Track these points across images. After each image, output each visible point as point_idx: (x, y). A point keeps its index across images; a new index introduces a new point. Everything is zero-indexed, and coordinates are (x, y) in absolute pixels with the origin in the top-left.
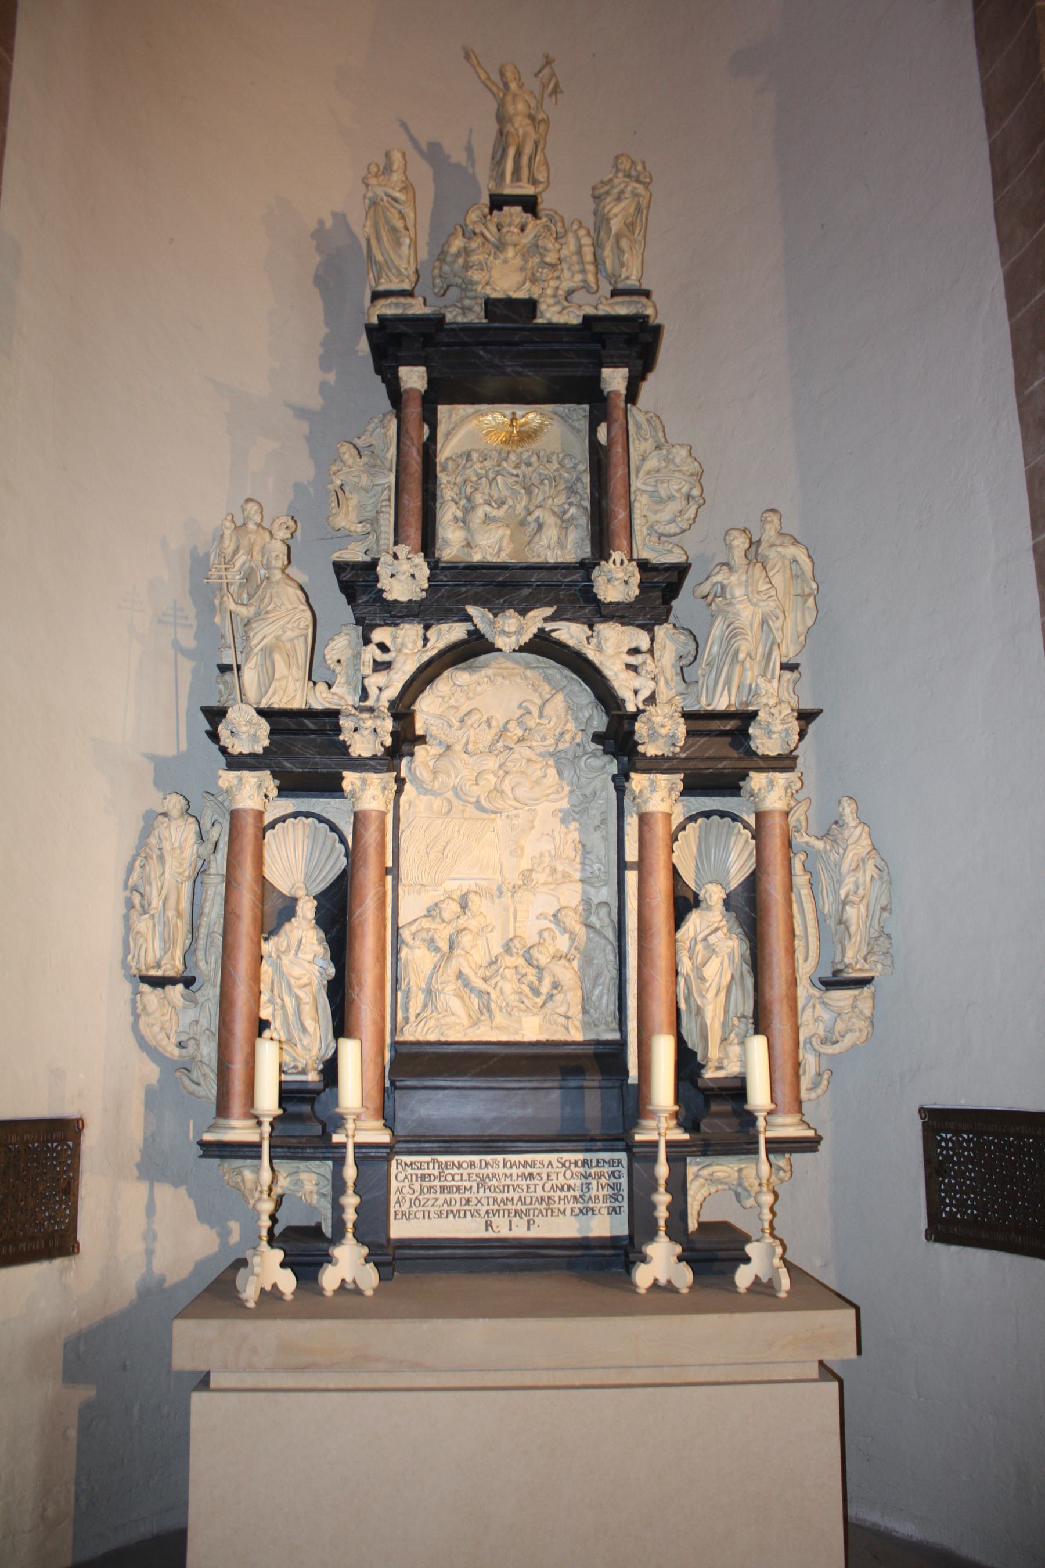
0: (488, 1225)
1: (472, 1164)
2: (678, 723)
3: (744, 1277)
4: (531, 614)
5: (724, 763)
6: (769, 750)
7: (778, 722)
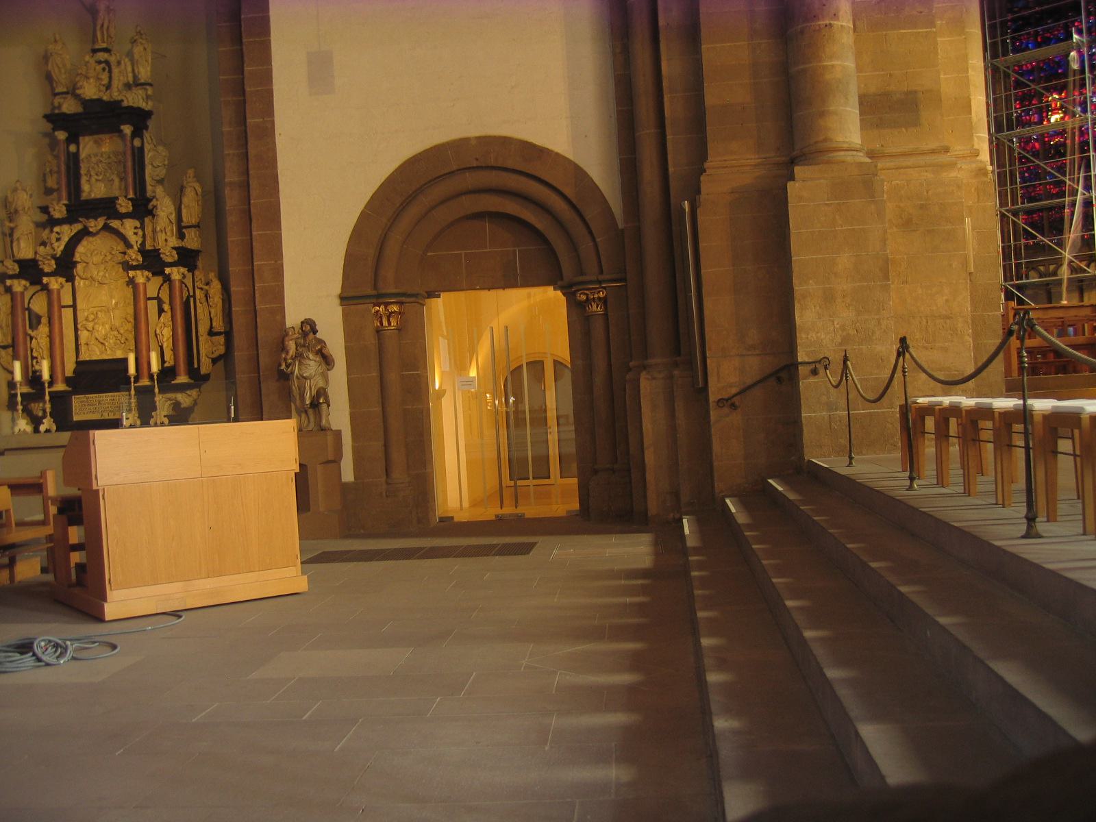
0: (102, 415)
1: (96, 397)
3: (152, 422)
4: (99, 219)
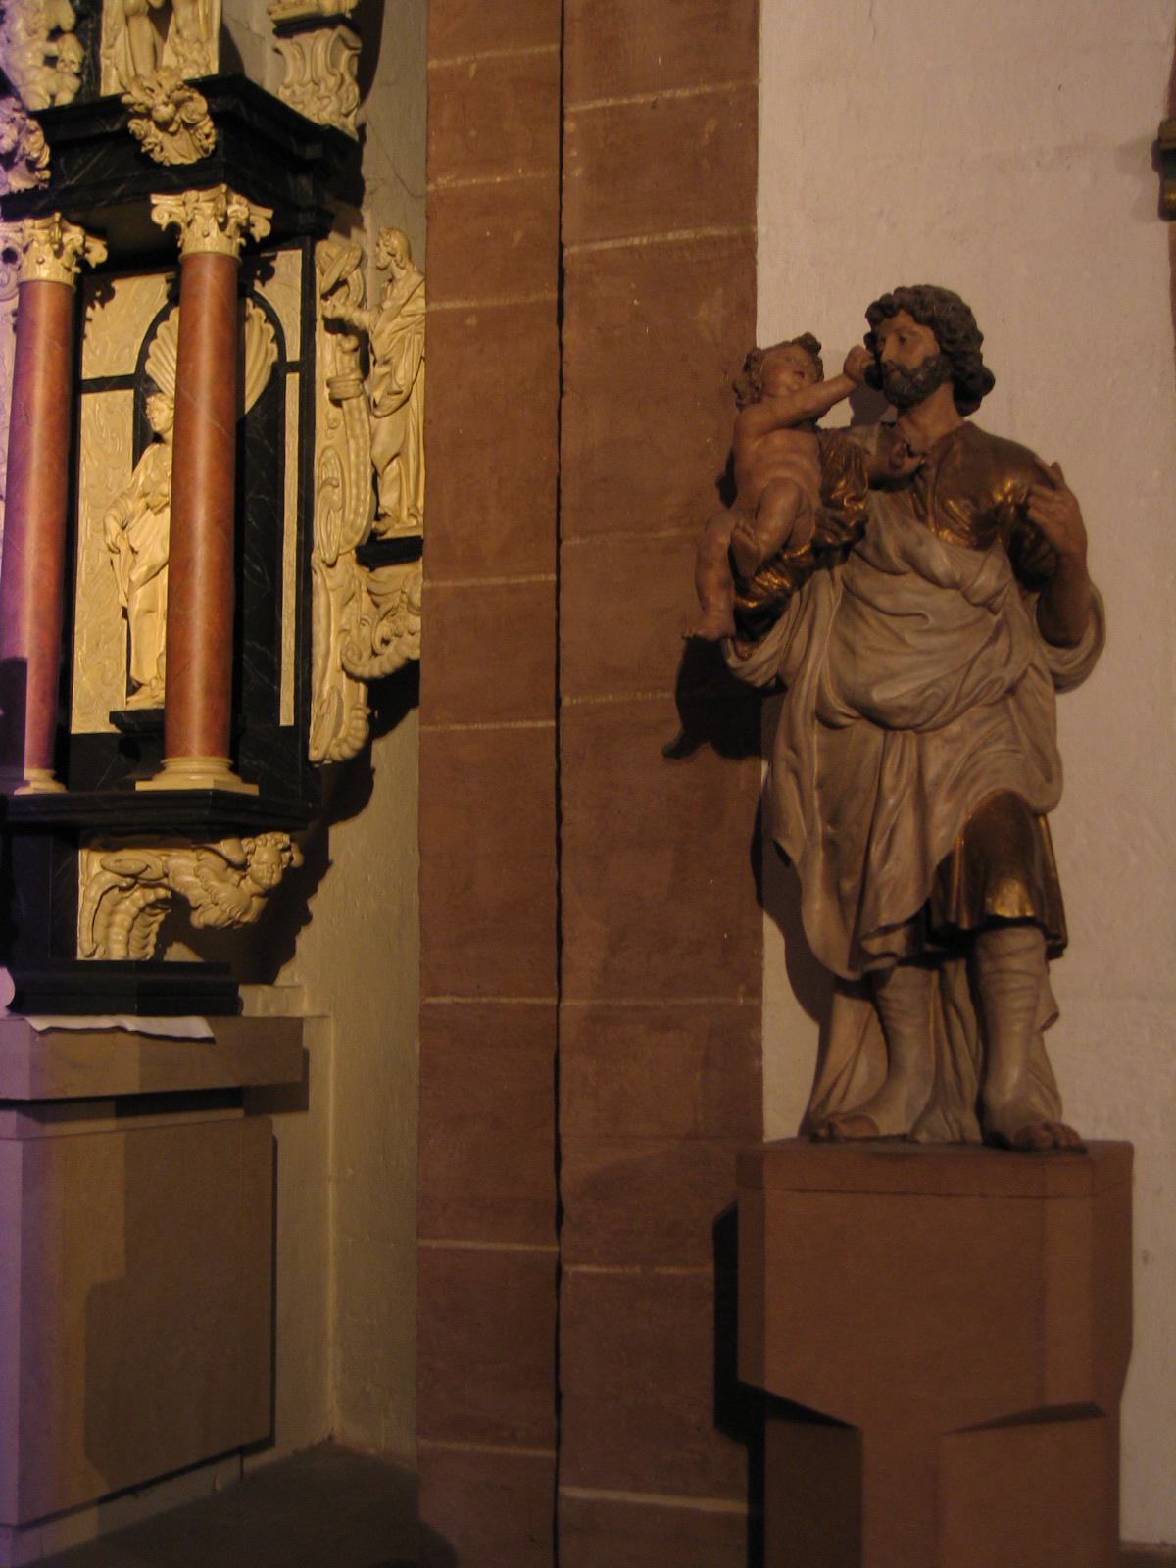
2: (32, 132)
5: (122, 187)
6: (183, 156)
7: (162, 98)
